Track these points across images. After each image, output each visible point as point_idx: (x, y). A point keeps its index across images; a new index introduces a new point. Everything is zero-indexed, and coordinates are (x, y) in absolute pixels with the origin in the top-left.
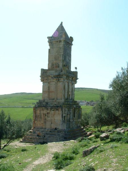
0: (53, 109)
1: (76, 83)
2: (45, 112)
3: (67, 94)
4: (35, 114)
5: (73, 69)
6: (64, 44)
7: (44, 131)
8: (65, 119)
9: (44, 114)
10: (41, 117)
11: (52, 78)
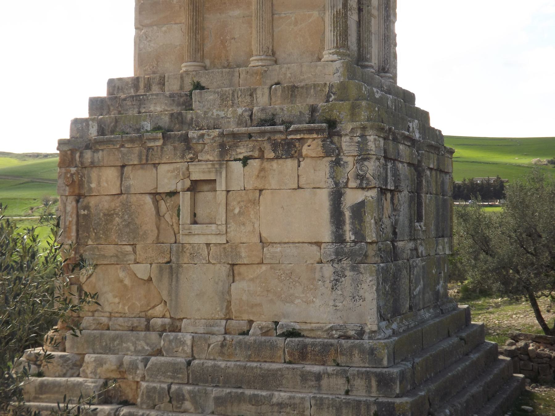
0: (243, 151)
2: (168, 176)
4: (79, 198)
7: (159, 353)
8: (360, 236)
9: (155, 195)
10: (132, 230)
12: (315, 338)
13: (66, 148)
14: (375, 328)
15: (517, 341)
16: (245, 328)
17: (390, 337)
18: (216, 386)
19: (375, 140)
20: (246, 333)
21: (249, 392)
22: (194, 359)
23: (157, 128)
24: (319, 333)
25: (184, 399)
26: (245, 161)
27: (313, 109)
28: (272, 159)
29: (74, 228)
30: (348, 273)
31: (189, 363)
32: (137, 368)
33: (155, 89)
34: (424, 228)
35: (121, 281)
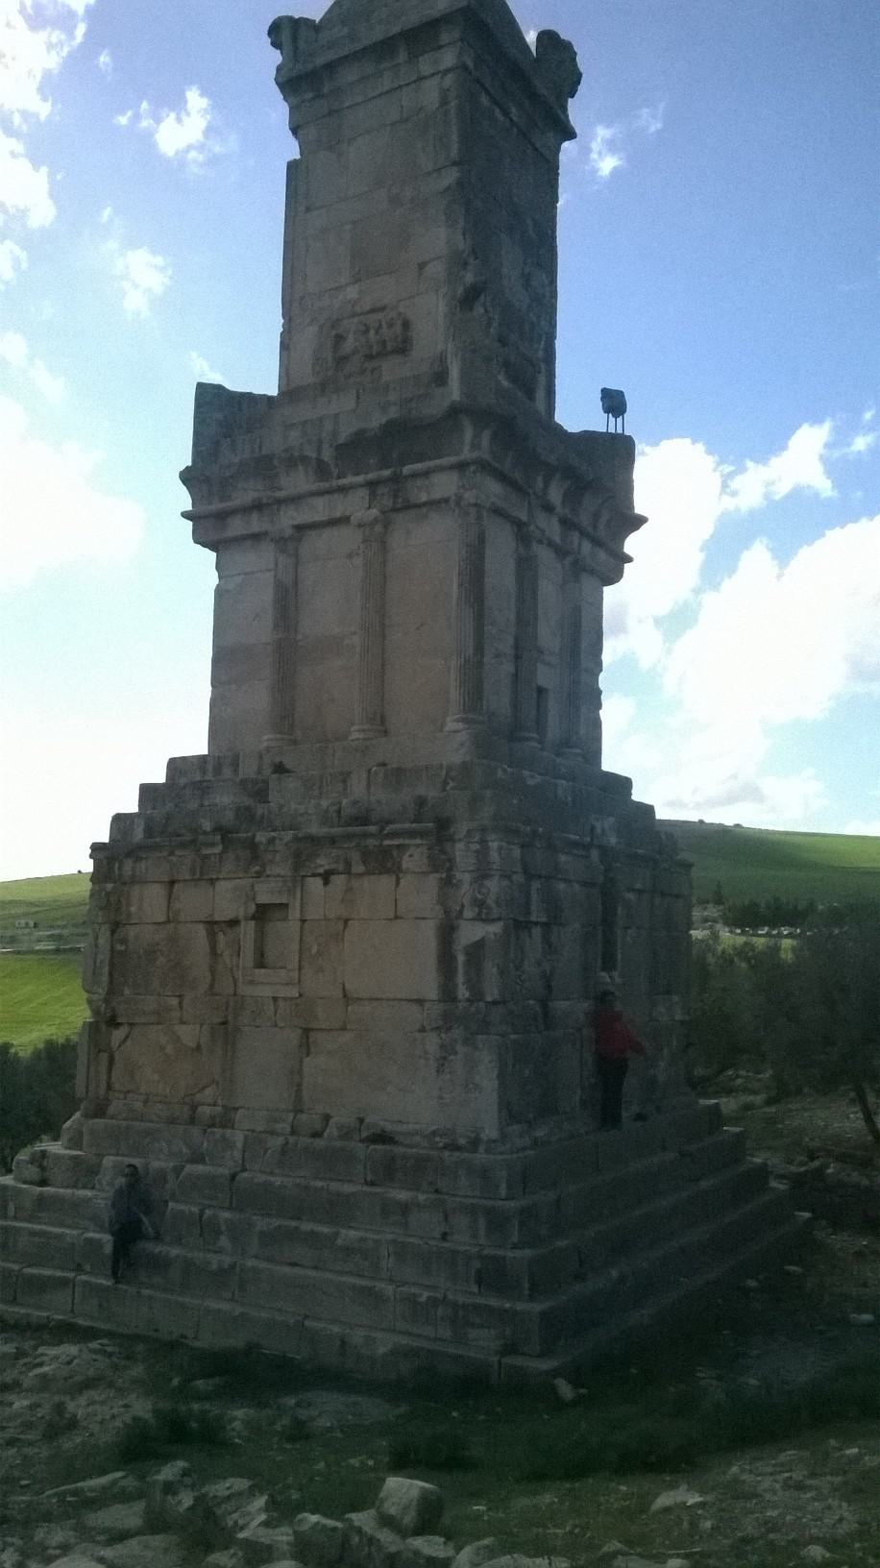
0: (323, 863)
1: (613, 576)
2: (227, 898)
3: (516, 676)
4: (115, 926)
5: (576, 410)
6: (471, 65)
7: (198, 1158)
8: (477, 995)
9: (211, 925)
11: (322, 470)
12: (411, 1147)
13: (101, 856)
14: (494, 1134)
15: (812, 1158)
16: (318, 1127)
17: (524, 1149)
18: (269, 1215)
19: (500, 848)
20: (317, 1135)
21: (306, 1226)
22: (244, 1170)
23: (218, 829)
24: (418, 1138)
25: (218, 1233)
26: (326, 877)
27: (421, 802)
28: (361, 875)
29: (106, 969)
30: (460, 1049)
31: (233, 1177)
32: (166, 1181)
33: (227, 772)
34: (618, 980)
35: (162, 1048)
